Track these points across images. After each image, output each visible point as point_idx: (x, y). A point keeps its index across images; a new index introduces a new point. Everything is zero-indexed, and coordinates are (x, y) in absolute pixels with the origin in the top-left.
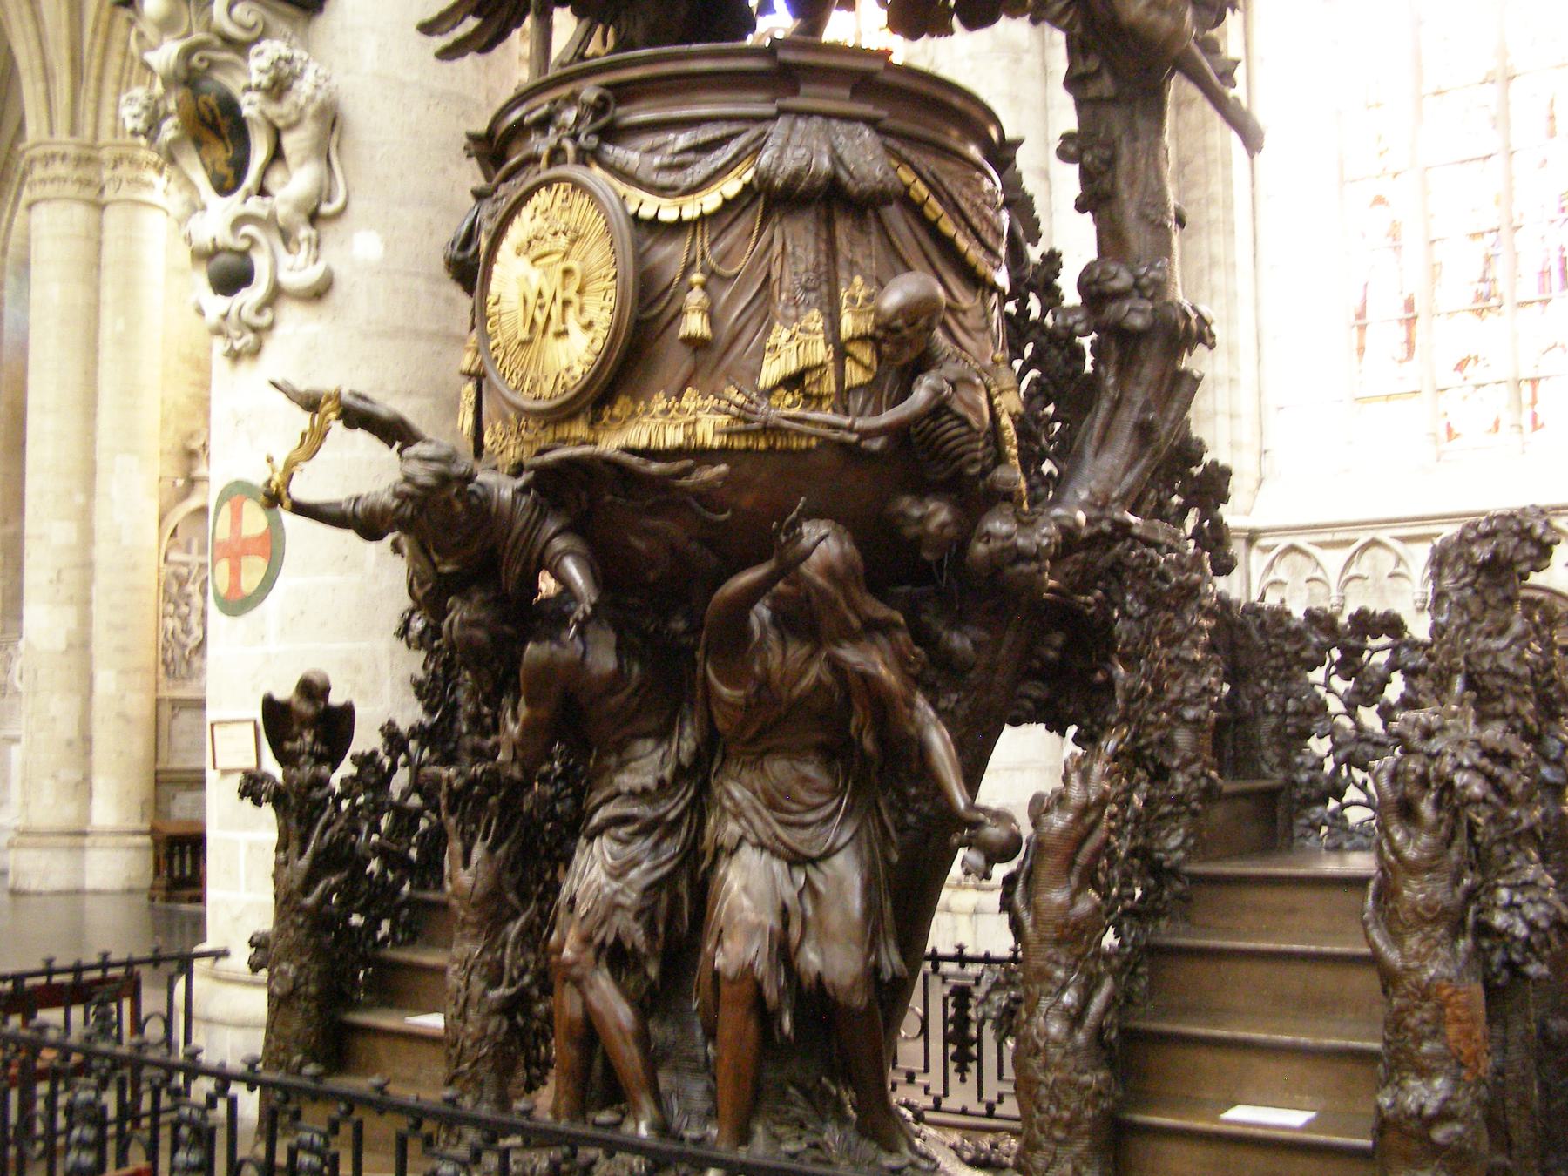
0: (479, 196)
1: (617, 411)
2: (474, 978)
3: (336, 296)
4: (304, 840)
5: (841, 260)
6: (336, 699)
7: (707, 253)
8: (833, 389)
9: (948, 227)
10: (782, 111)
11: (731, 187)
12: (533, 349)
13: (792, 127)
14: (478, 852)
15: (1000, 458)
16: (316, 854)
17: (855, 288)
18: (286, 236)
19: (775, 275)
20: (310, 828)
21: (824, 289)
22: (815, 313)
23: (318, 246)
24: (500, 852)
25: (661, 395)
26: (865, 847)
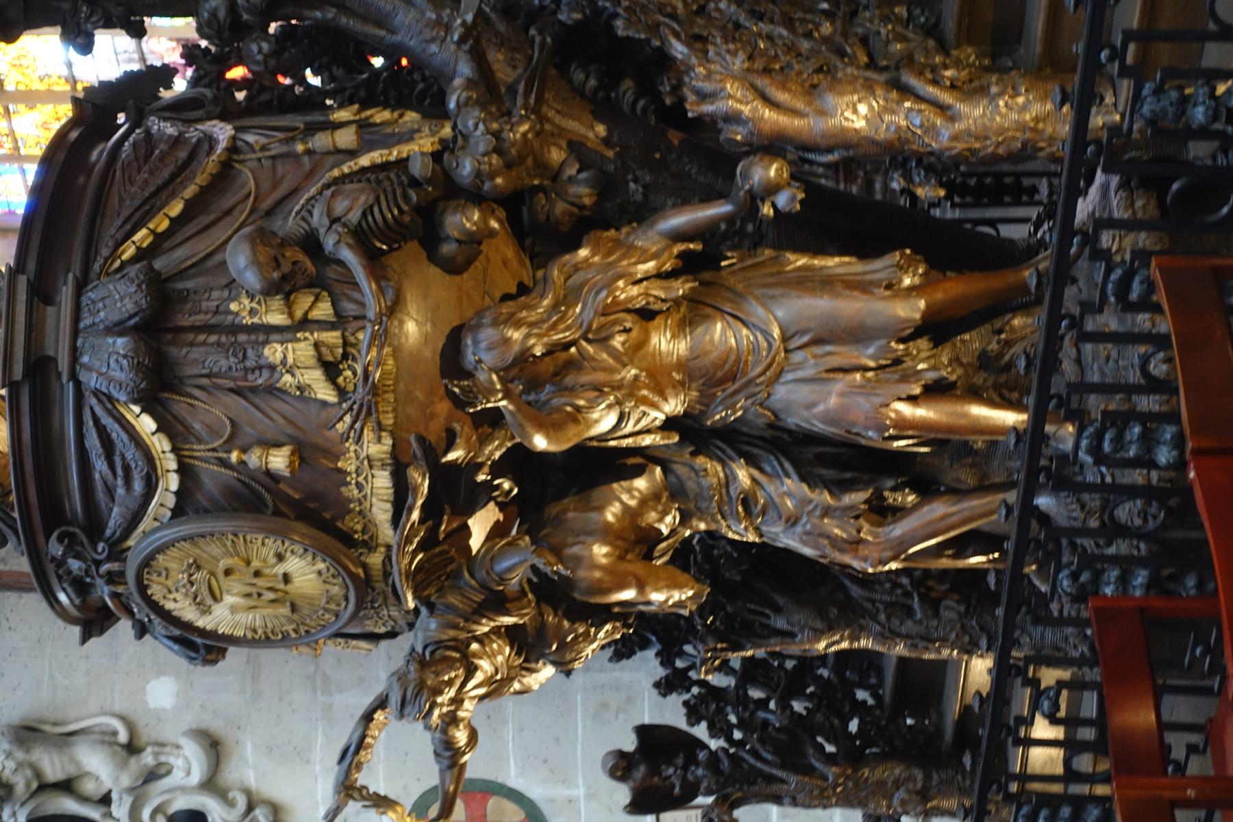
0: (142, 630)
1: (359, 527)
2: (903, 630)
3: (216, 725)
4: (770, 779)
5: (213, 321)
6: (629, 743)
7: (210, 446)
8: (337, 334)
9: (176, 208)
10: (73, 376)
11: (146, 424)
12: (298, 602)
13: (89, 369)
14: (780, 623)
15: (402, 163)
16: (783, 766)
17: (241, 307)
18: (152, 776)
19: (231, 384)
20: (760, 773)
21: (242, 338)
22: (267, 352)
23: (162, 745)
24: (781, 601)
25: (343, 489)
26: (772, 292)
